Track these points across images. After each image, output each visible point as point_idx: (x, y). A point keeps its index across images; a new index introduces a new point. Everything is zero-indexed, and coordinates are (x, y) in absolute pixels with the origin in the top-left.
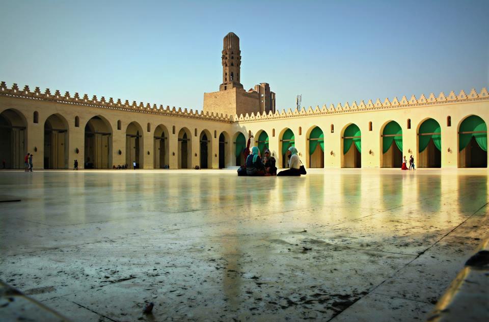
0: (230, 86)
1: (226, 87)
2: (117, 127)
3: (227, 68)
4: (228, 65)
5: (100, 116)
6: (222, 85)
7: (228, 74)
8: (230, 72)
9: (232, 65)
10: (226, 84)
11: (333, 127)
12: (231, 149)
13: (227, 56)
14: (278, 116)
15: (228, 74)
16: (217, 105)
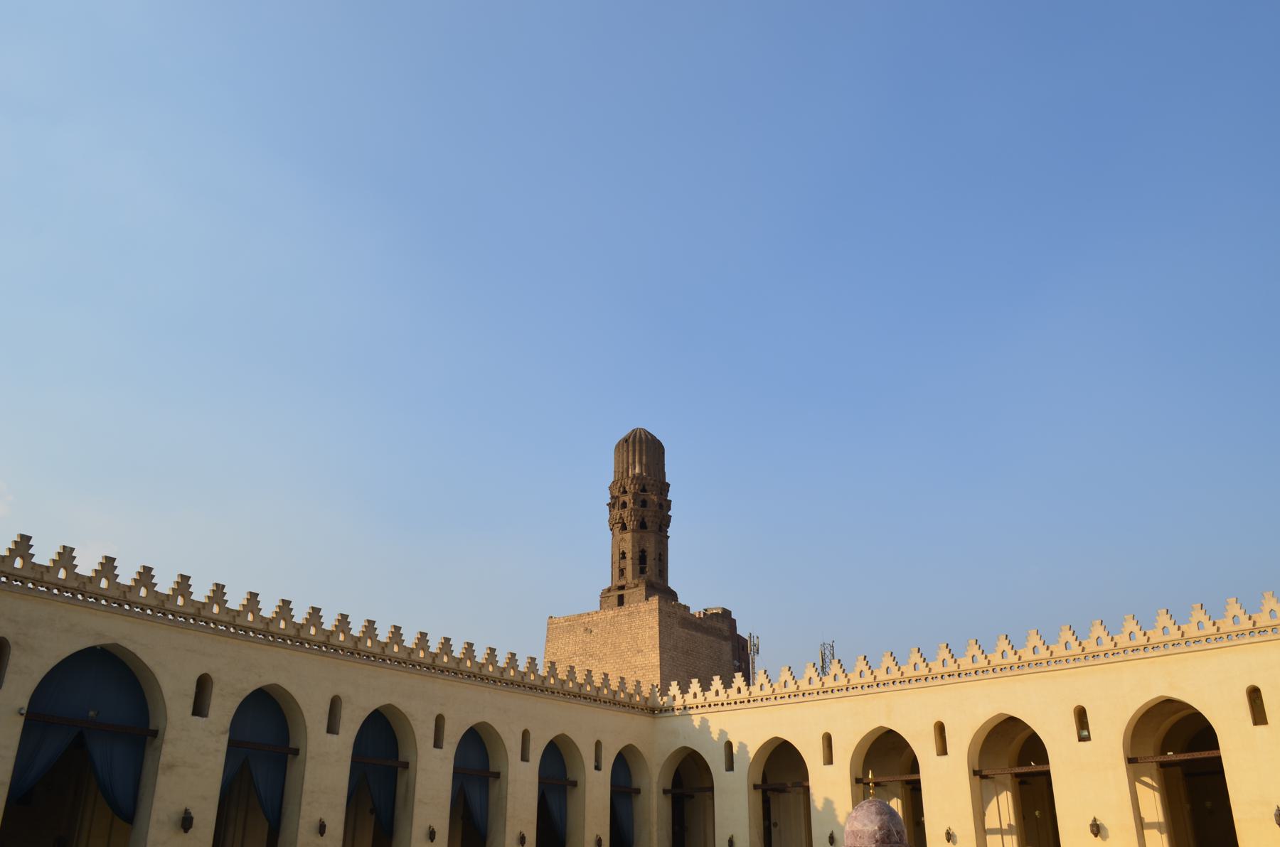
0: (636, 594)
1: (621, 601)
2: (190, 701)
3: (628, 536)
4: (630, 526)
5: (117, 646)
6: (609, 590)
7: (629, 556)
8: (637, 550)
9: (642, 525)
10: (622, 588)
11: (1081, 716)
12: (654, 818)
13: (628, 498)
14: (842, 681)
15: (629, 556)
16: (591, 656)
